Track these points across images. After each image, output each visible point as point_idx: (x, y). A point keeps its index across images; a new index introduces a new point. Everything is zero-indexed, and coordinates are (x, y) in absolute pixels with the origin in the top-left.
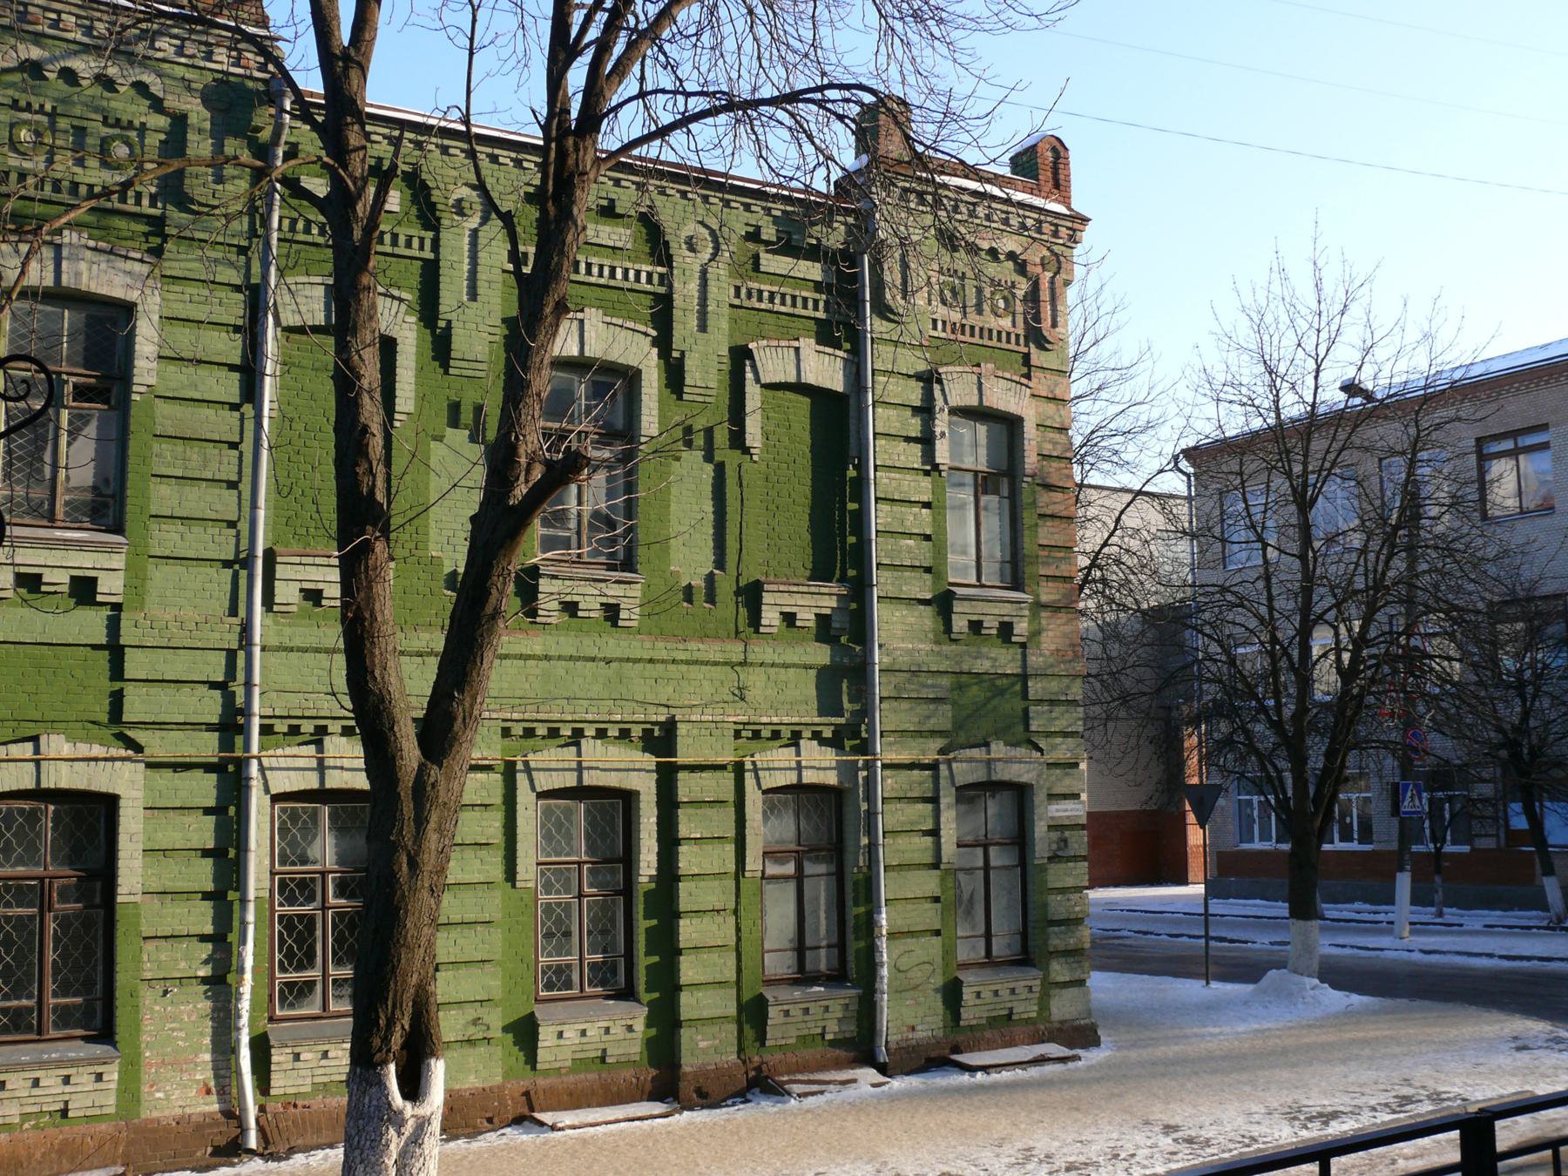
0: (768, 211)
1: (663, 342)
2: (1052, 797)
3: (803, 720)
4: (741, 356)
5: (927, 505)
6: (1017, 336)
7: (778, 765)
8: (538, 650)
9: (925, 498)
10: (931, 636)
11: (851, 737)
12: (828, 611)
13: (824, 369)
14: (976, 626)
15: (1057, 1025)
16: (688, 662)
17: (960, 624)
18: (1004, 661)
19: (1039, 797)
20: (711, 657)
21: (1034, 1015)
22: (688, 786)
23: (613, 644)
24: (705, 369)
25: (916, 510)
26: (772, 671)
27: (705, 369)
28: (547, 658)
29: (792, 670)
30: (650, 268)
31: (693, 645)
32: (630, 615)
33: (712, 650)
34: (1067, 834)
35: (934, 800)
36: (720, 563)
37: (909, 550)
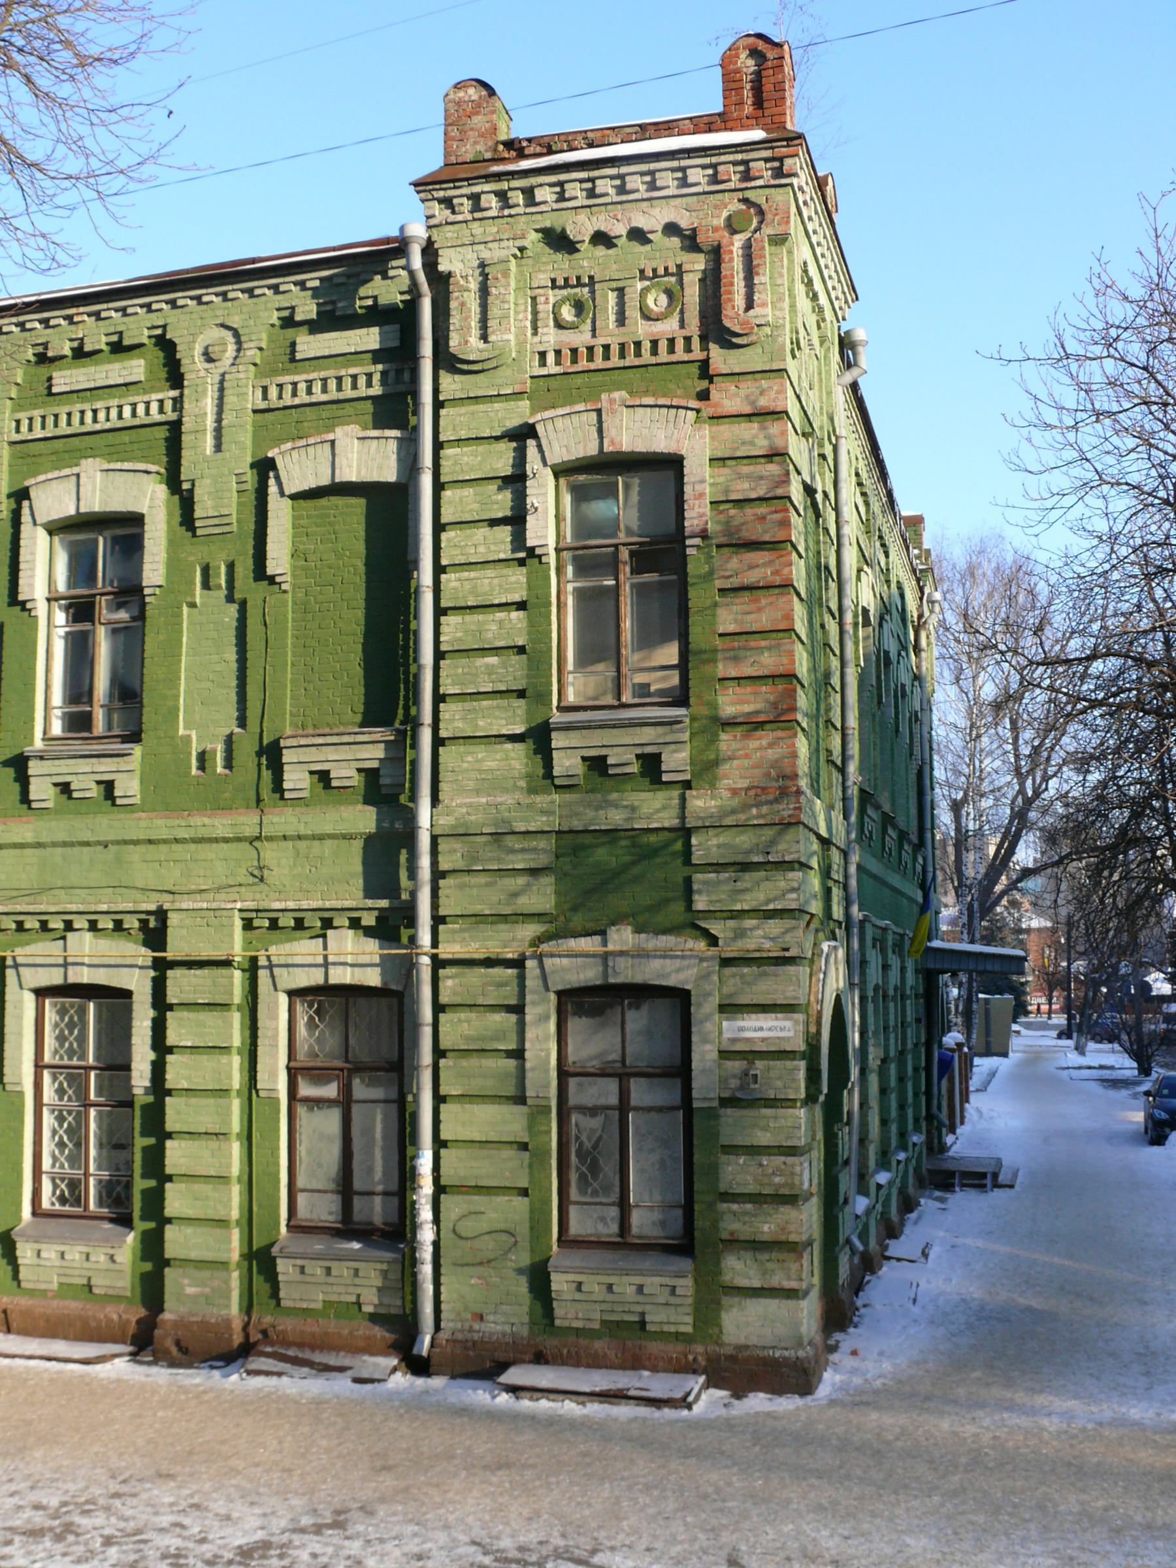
0: (302, 285)
1: (173, 480)
2: (729, 1008)
3: (328, 905)
4: (265, 467)
5: (521, 606)
6: (688, 339)
7: (300, 961)
8: (29, 837)
9: (517, 598)
10: (522, 784)
11: (392, 926)
12: (375, 764)
13: (368, 457)
14: (597, 765)
15: (728, 1351)
16: (195, 841)
17: (566, 763)
18: (654, 809)
19: (704, 1010)
20: (221, 832)
21: (689, 1329)
22: (179, 984)
23: (106, 825)
24: (220, 497)
25: (500, 615)
26: (302, 845)
27: (220, 497)
28: (39, 845)
29: (328, 843)
30: (160, 396)
31: (197, 820)
32: (129, 787)
33: (220, 825)
34: (759, 1064)
35: (518, 1009)
36: (242, 722)
37: (490, 670)
